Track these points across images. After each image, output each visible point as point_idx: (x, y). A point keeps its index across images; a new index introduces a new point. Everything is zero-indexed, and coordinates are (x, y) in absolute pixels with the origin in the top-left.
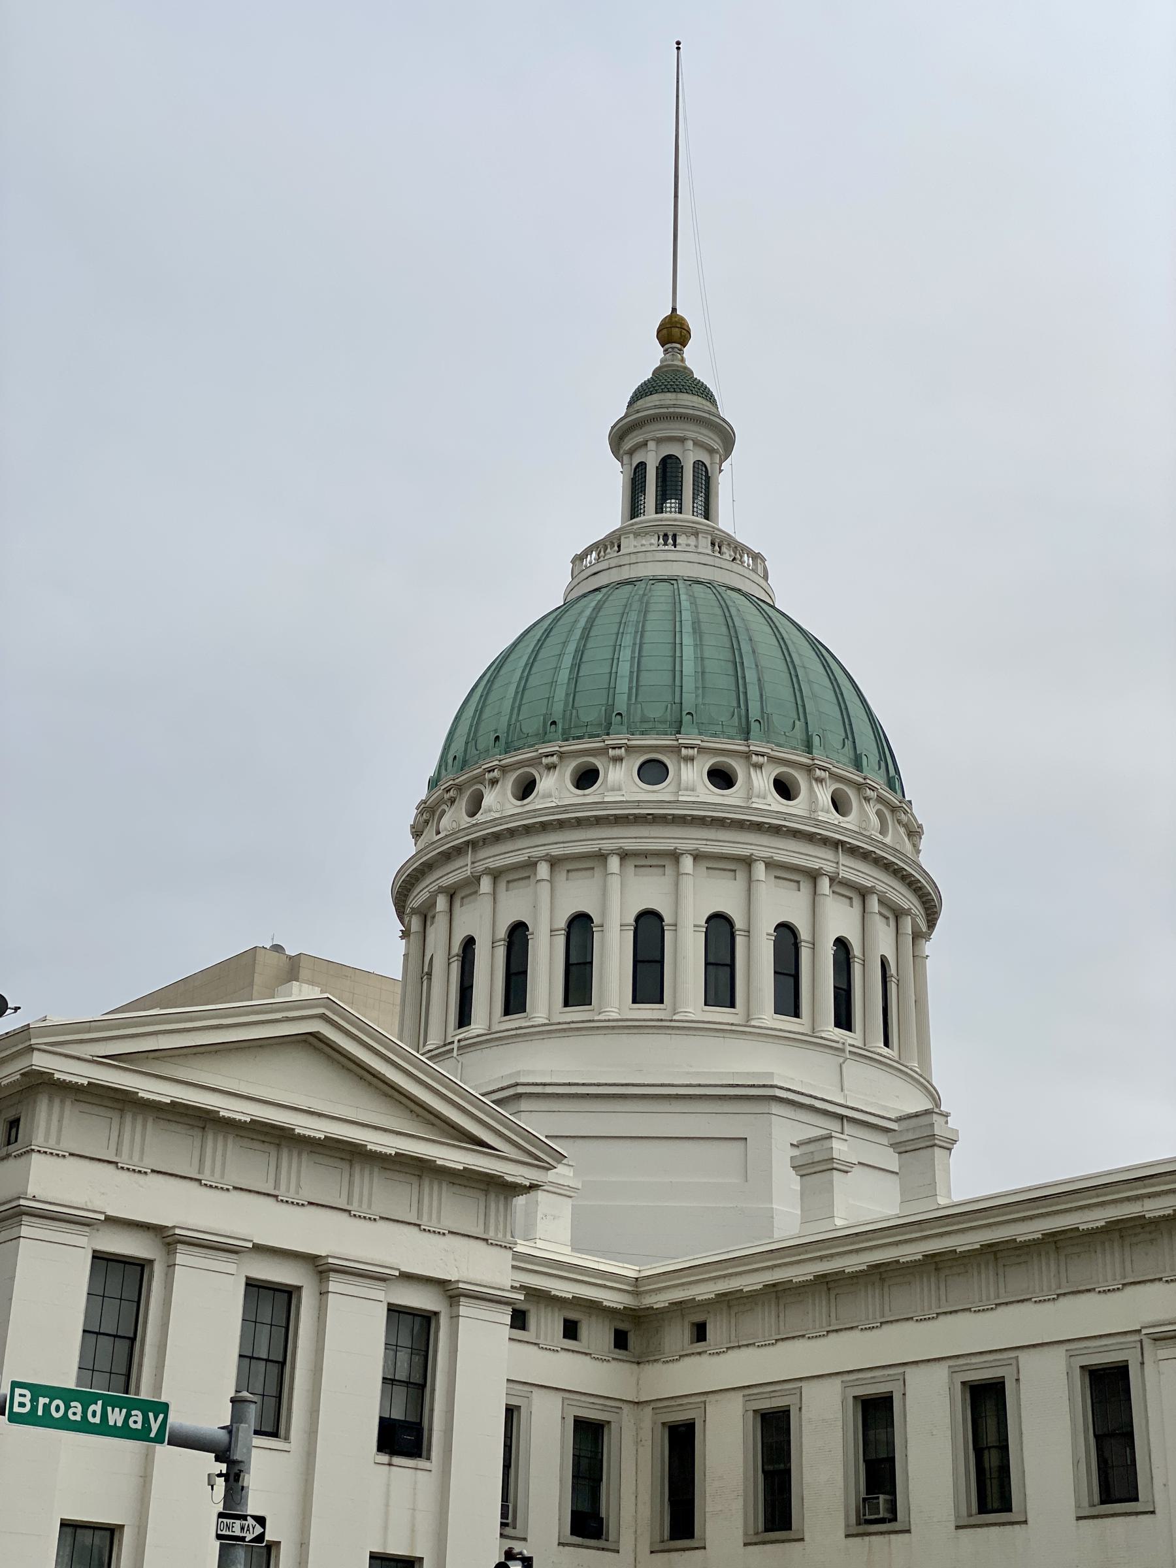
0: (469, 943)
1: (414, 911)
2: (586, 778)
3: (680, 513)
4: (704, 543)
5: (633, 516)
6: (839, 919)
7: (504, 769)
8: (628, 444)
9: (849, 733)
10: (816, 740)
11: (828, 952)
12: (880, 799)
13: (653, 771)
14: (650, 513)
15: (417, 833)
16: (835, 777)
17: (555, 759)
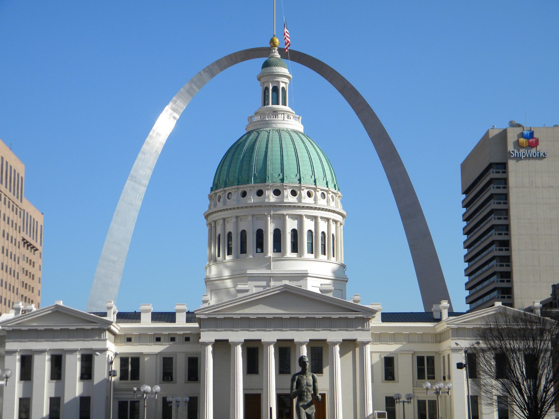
0: (230, 234)
1: (213, 221)
2: (260, 193)
3: (278, 104)
4: (286, 116)
5: (265, 105)
6: (323, 226)
7: (238, 188)
8: (263, 80)
9: (325, 176)
10: (317, 180)
11: (320, 235)
12: (332, 192)
13: (277, 192)
14: (270, 105)
15: (210, 197)
16: (322, 190)
17: (252, 188)
